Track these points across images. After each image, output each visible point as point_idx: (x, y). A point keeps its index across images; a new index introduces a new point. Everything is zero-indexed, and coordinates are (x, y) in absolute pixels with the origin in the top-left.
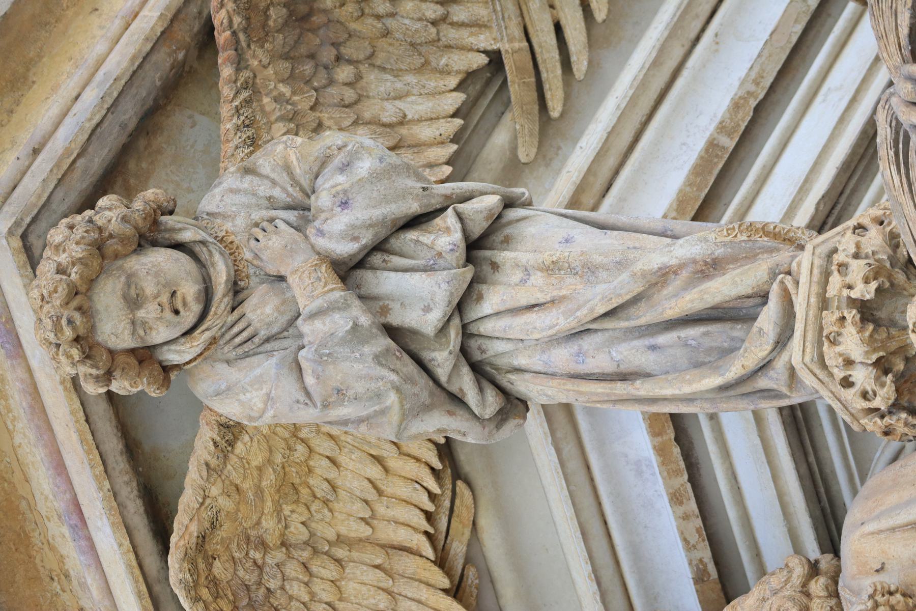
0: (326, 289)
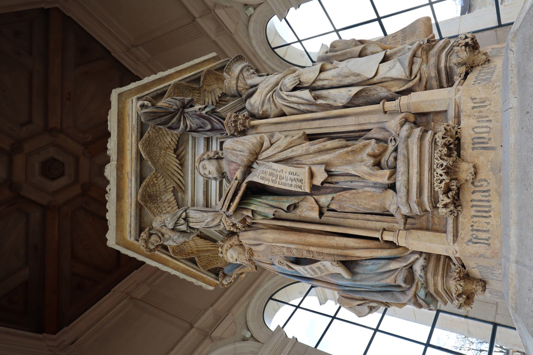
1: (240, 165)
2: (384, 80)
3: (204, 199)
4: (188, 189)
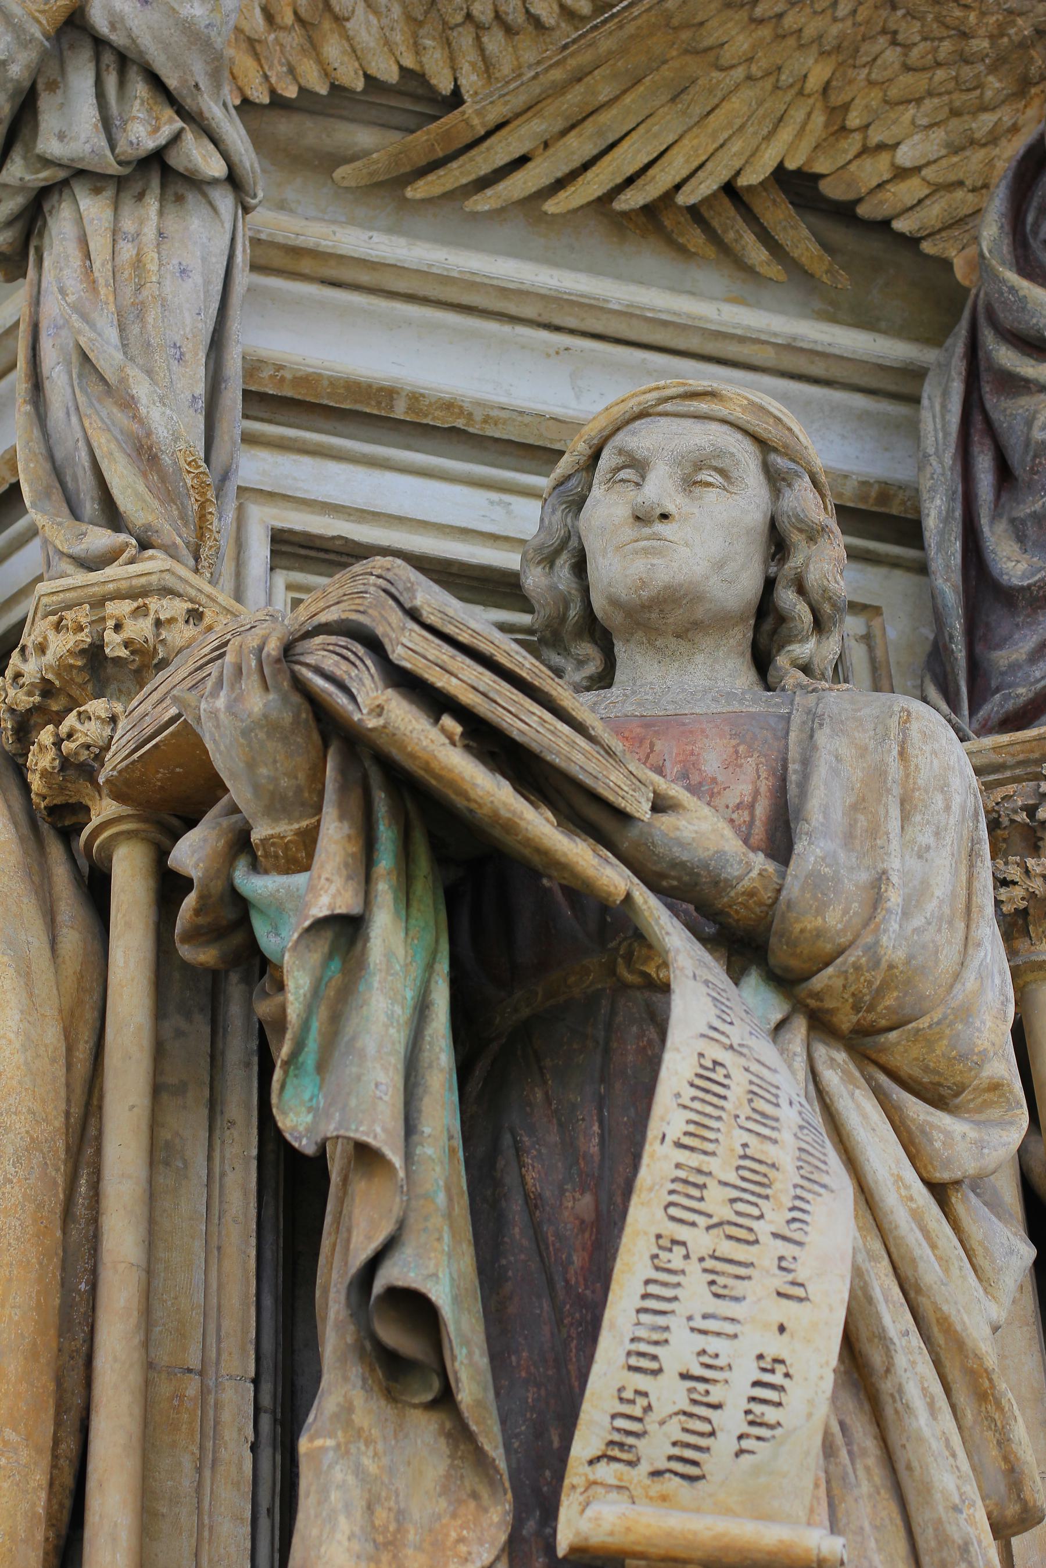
0: (37, 14)
3: (306, 380)
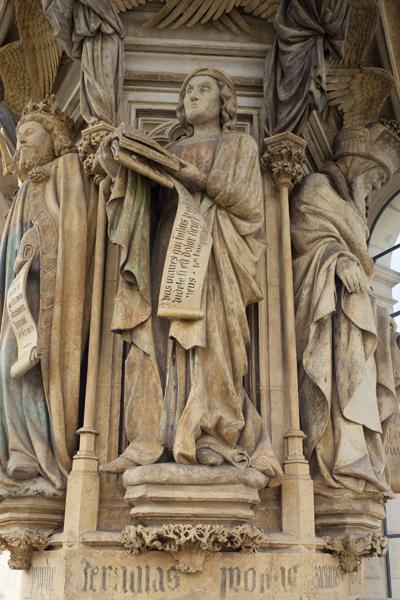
1: (208, 172)
2: (337, 432)
3: (140, 76)
4: (160, 37)
